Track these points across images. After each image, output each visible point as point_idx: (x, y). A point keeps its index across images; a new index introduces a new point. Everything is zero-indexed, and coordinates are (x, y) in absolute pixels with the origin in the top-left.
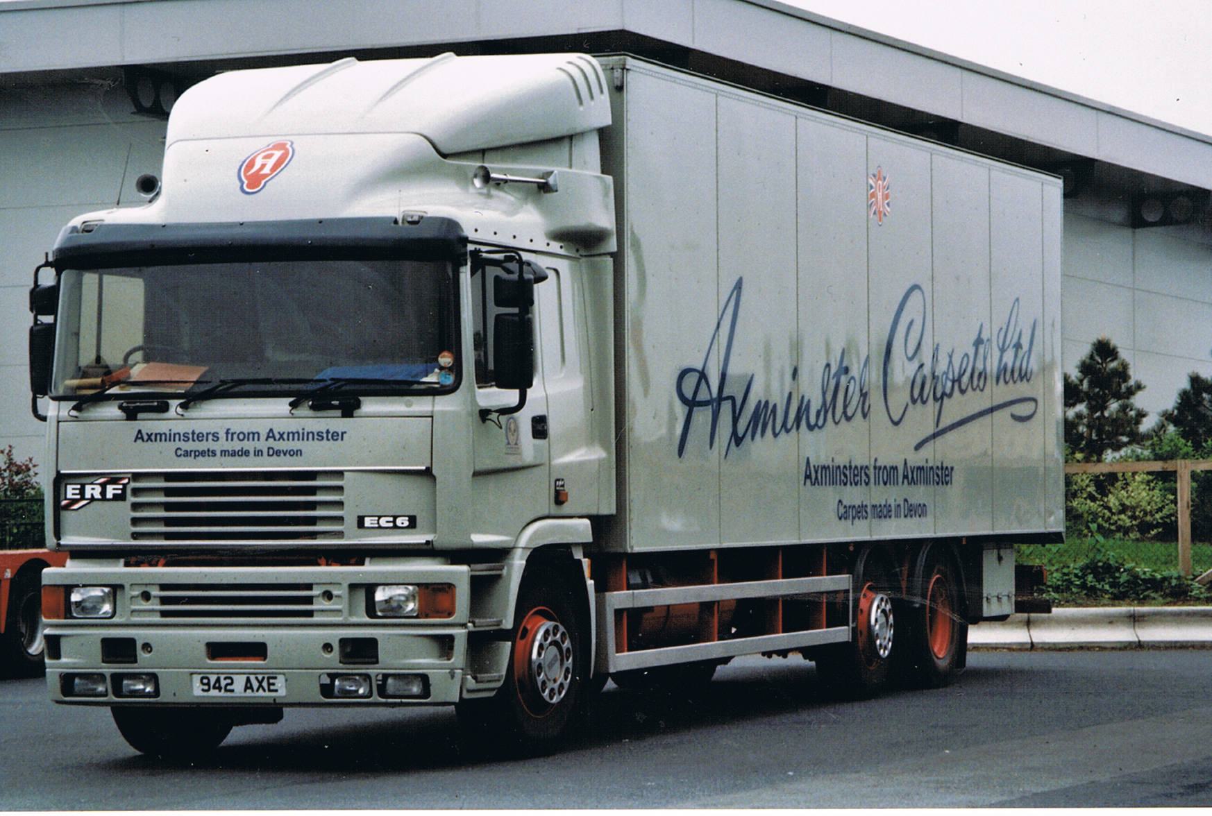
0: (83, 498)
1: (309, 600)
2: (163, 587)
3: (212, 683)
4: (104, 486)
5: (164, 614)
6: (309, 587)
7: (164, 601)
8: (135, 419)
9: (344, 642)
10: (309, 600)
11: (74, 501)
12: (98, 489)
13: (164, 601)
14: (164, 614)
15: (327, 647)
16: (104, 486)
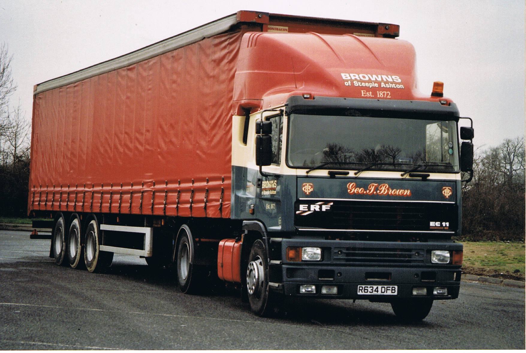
0: (309, 210)
1: (410, 256)
2: (348, 249)
3: (374, 290)
4: (321, 206)
5: (347, 260)
6: (410, 250)
7: (347, 254)
8: (334, 178)
9: (423, 273)
10: (410, 256)
11: (305, 212)
12: (318, 207)
13: (347, 254)
14: (347, 260)
15: (417, 275)
16: (321, 206)
